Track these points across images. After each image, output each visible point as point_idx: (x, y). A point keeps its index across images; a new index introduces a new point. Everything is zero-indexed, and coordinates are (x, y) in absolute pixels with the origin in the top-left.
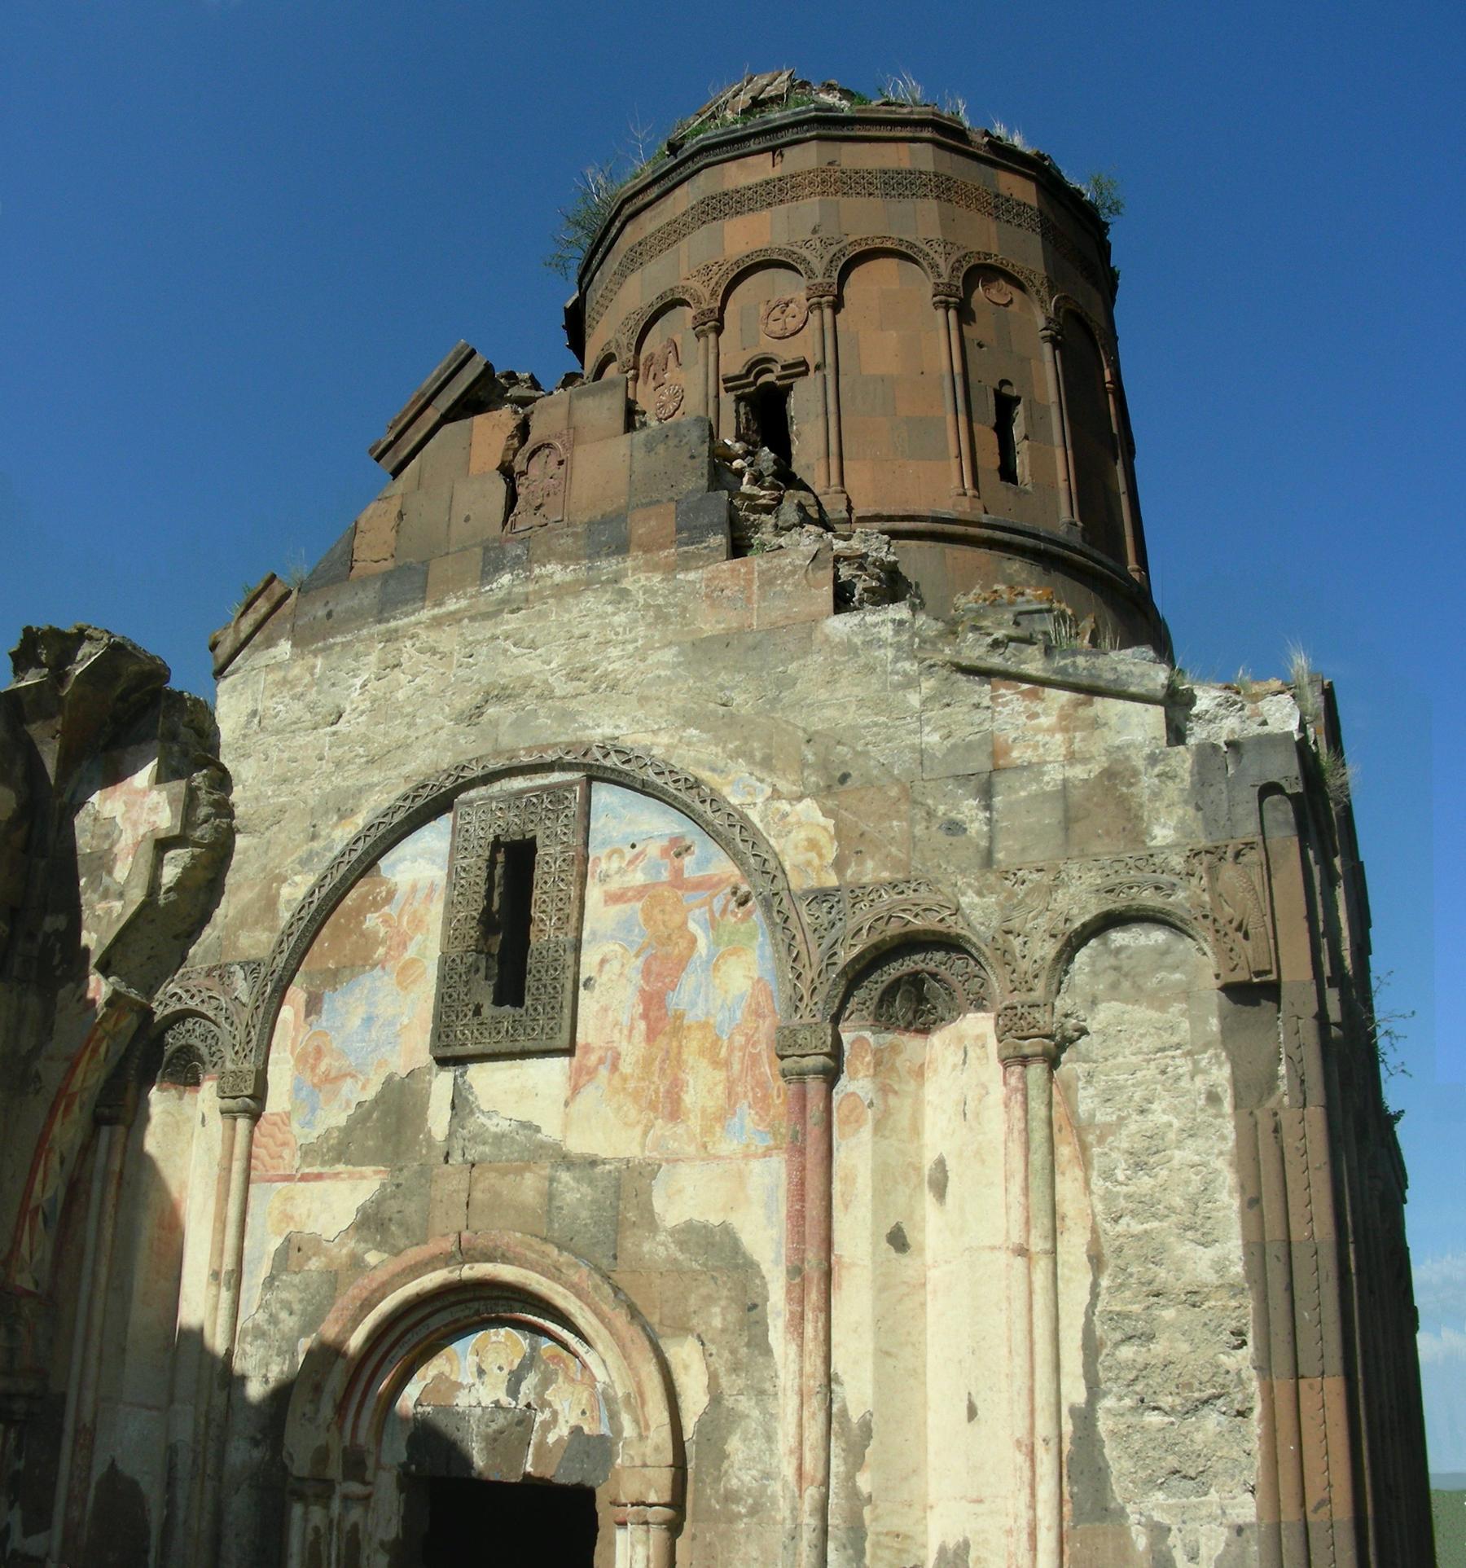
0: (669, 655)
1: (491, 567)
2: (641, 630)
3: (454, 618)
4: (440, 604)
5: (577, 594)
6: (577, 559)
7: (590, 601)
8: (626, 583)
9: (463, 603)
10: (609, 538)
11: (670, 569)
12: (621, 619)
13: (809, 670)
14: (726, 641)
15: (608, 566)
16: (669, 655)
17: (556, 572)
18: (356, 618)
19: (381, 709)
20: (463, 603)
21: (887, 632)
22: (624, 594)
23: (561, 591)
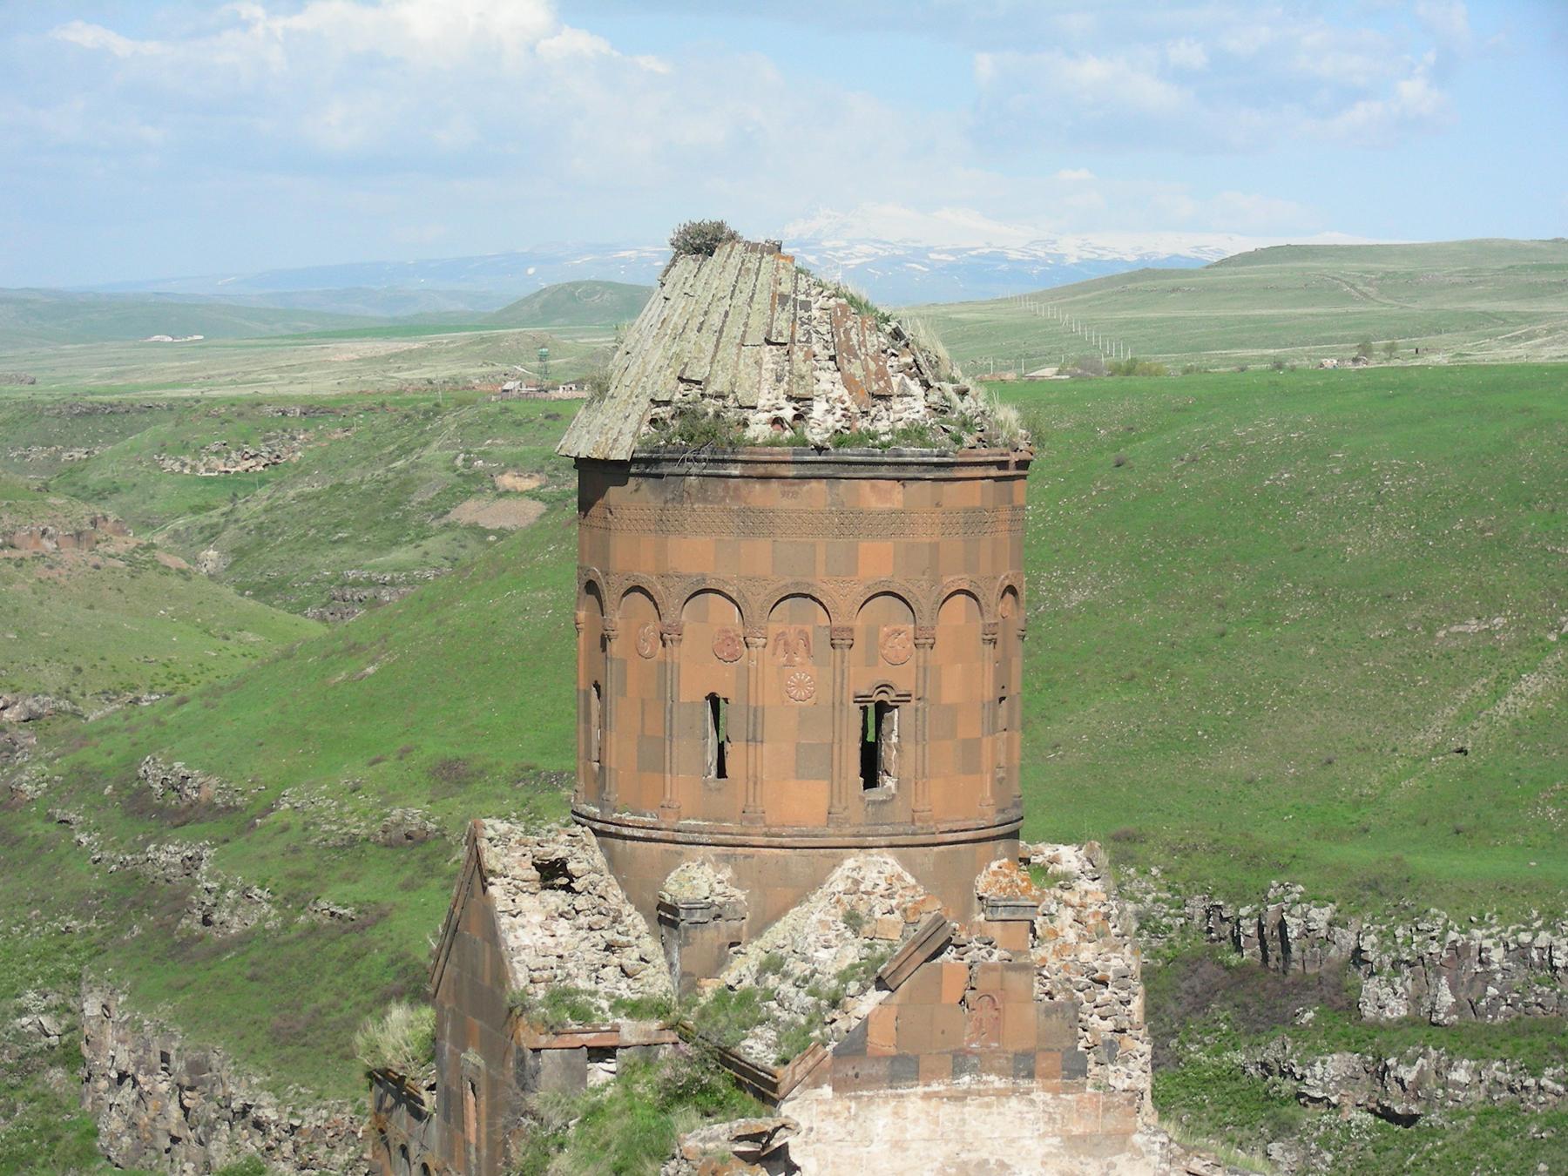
0: (1056, 1141)
1: (957, 1071)
2: (1041, 1125)
3: (936, 1094)
4: (928, 1085)
5: (1008, 1097)
6: (1007, 1076)
7: (1014, 1103)
8: (1033, 1096)
9: (942, 1088)
10: (1024, 1066)
11: (1056, 1092)
12: (1031, 1116)
13: (1121, 1160)
14: (1083, 1138)
15: (1024, 1084)
16: (1056, 1141)
17: (996, 1081)
18: (873, 1082)
19: (898, 1145)
20: (942, 1088)
21: (1157, 1147)
22: (1032, 1102)
23: (999, 1094)
